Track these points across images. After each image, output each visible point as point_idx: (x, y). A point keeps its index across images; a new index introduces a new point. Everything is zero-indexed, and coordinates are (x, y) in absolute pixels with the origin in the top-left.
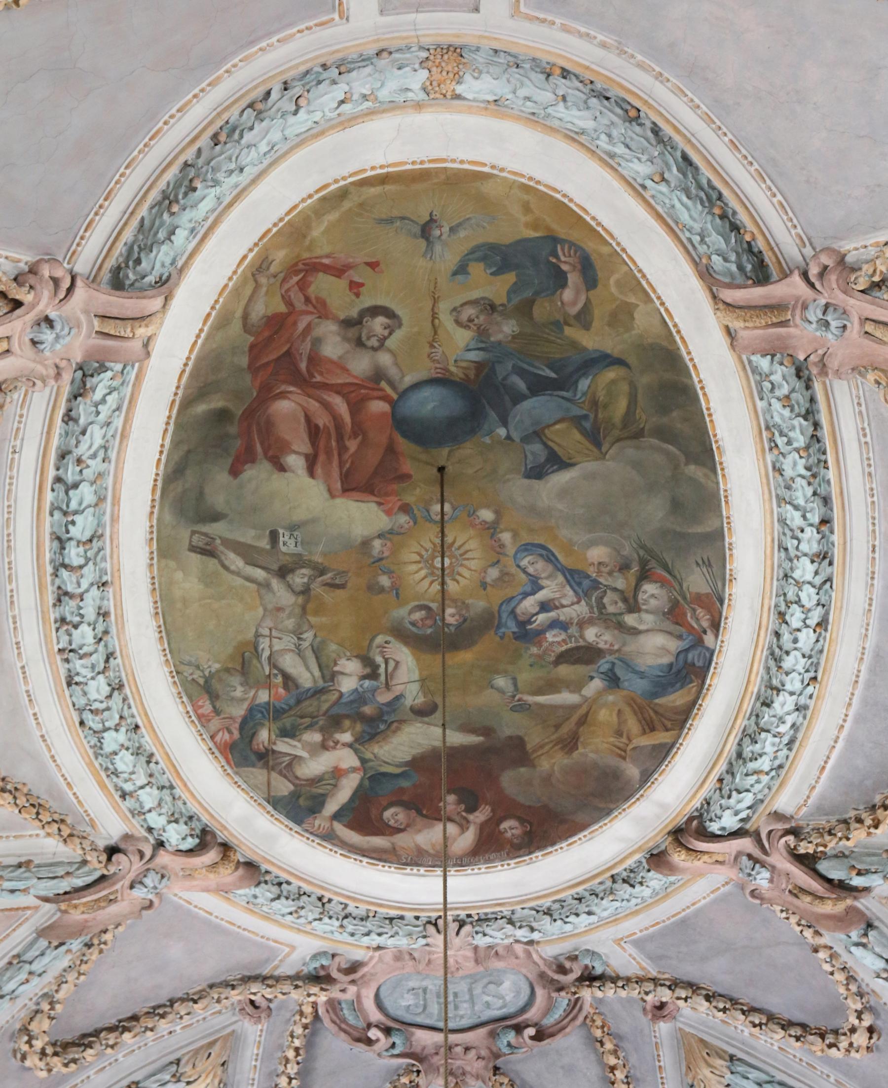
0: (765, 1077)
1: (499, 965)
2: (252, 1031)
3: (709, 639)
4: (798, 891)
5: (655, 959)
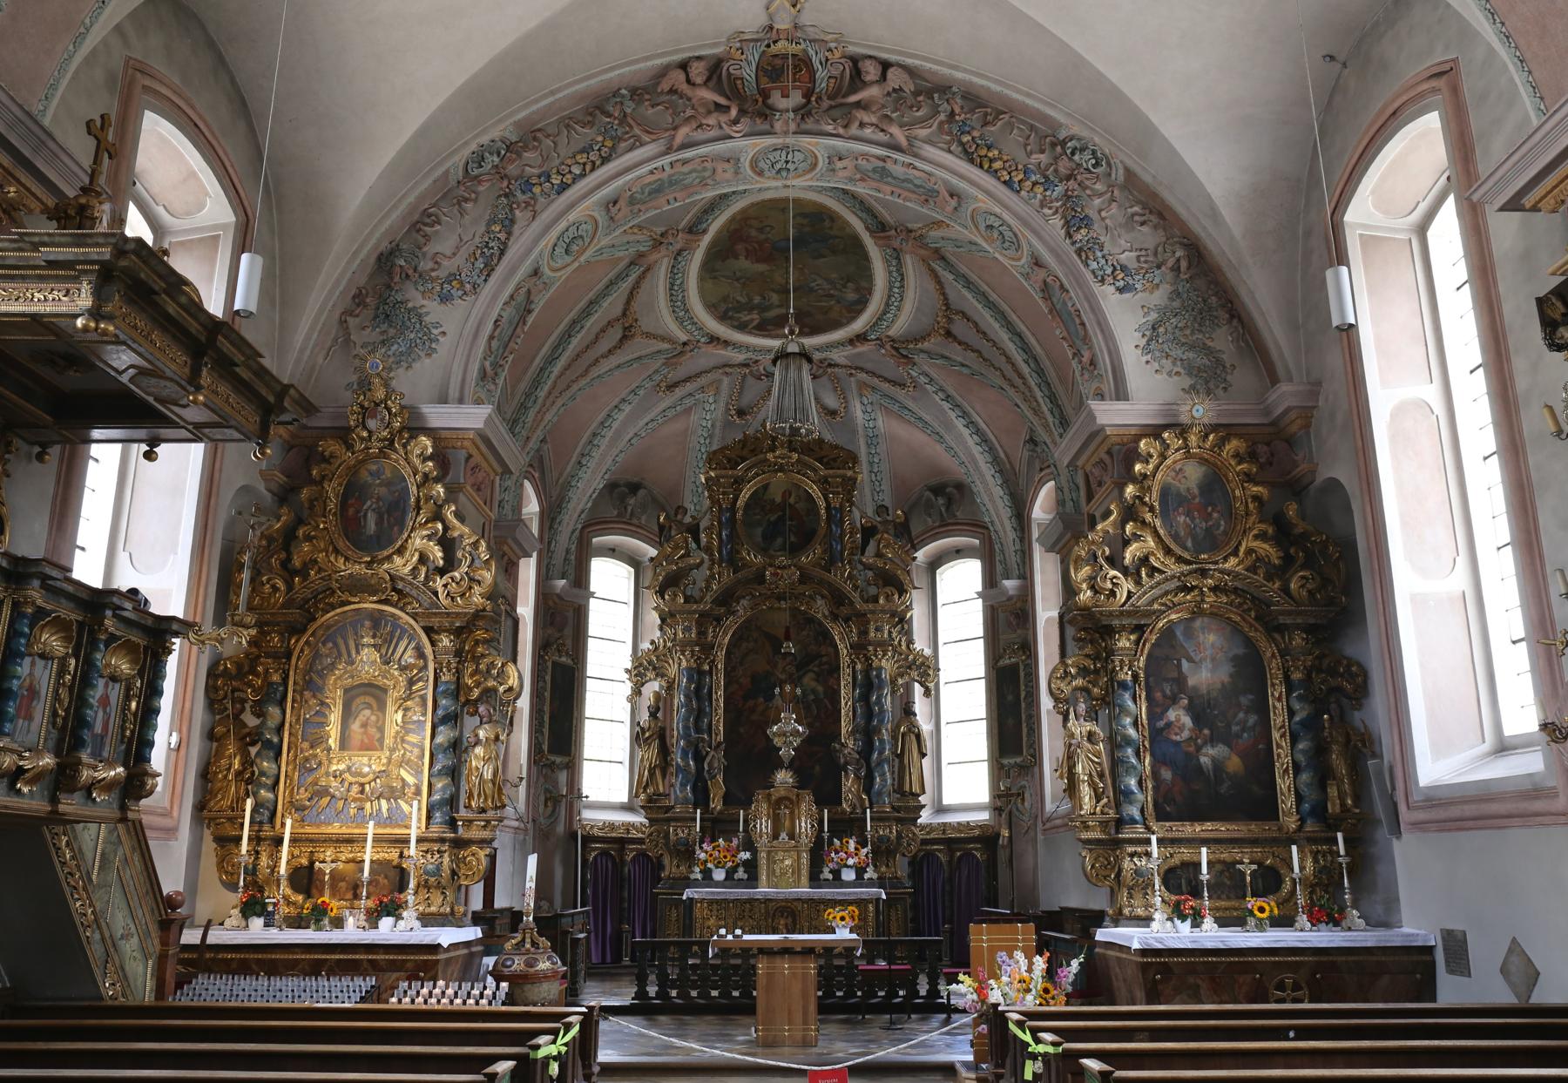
2: (726, 380)
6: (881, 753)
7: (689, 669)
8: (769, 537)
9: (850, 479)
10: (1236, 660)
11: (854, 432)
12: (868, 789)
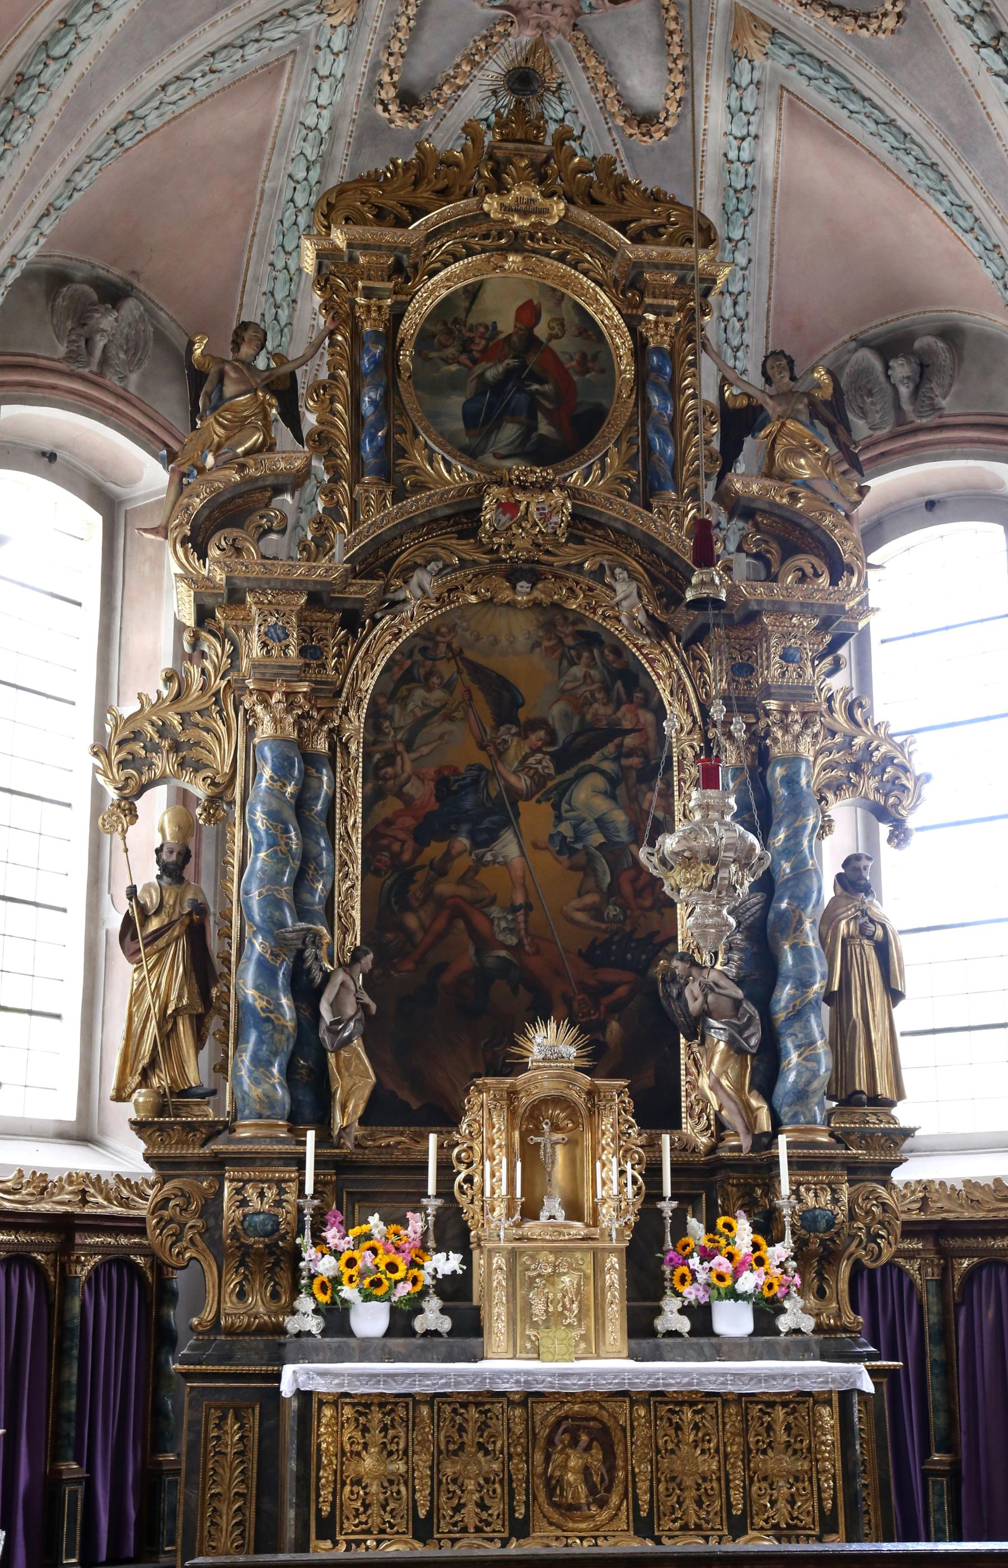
0: (798, 49)
6: (803, 984)
7: (279, 741)
8: (481, 421)
11: (695, 176)
12: (766, 1080)
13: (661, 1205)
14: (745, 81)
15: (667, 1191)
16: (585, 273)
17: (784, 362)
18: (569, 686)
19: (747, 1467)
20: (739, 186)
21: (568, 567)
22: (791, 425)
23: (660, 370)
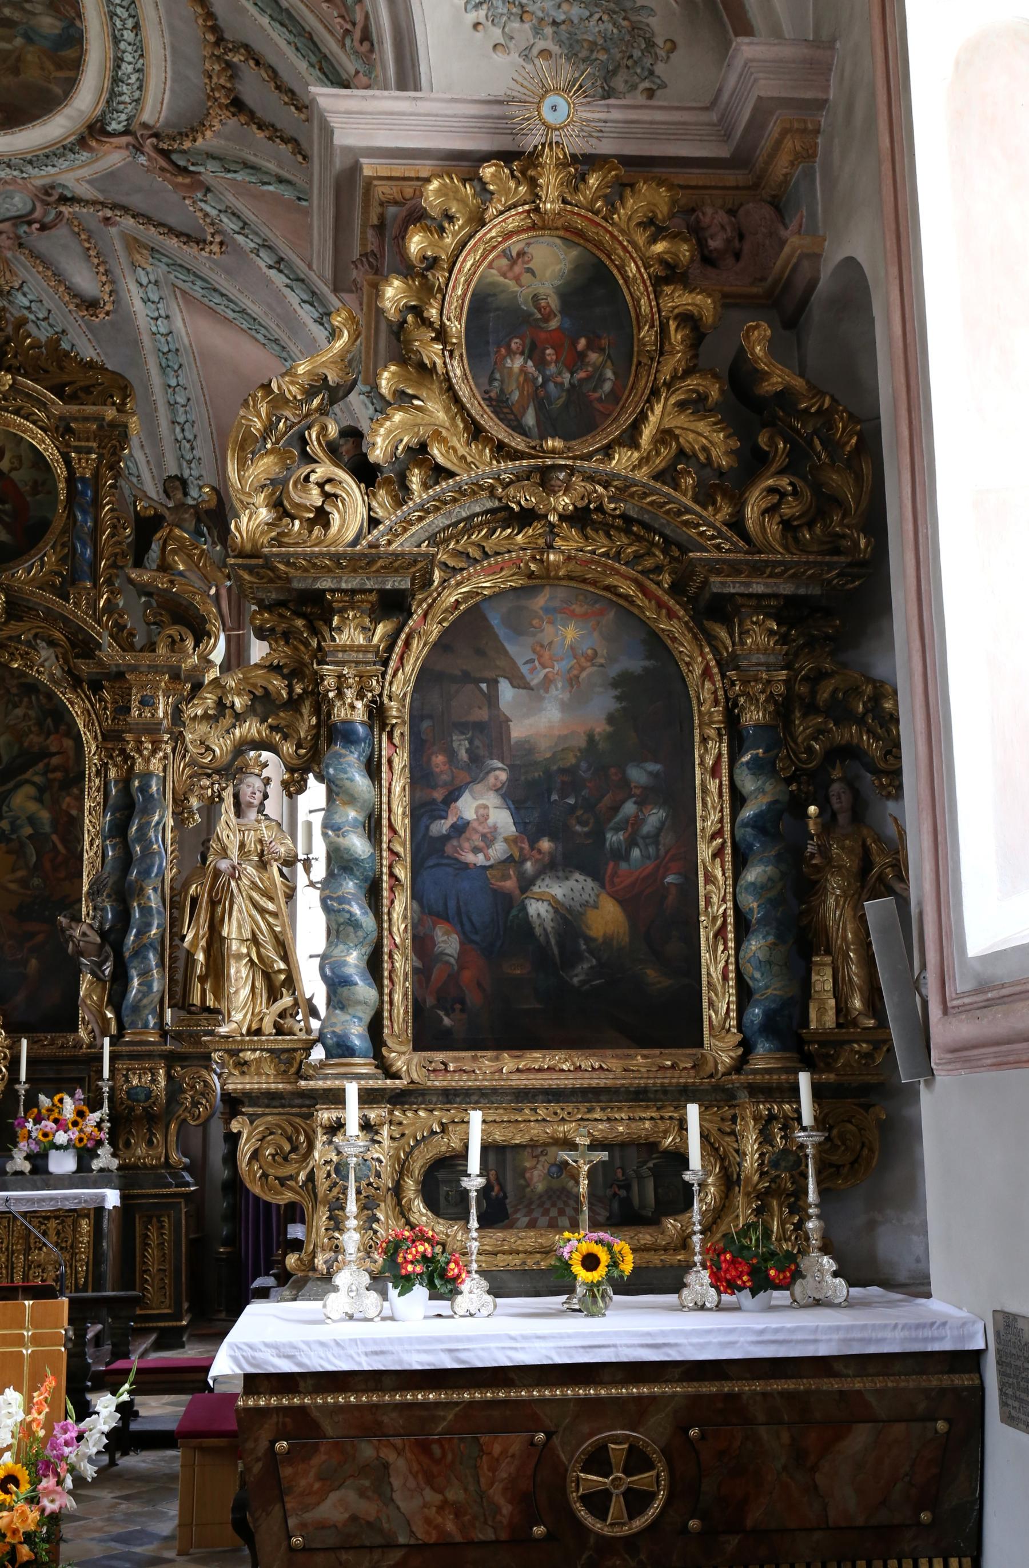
1: (11, 188)
3: (78, 23)
4: (162, 169)
5: (101, 191)
6: (141, 933)
9: (113, 425)
10: (623, 683)
11: (136, 344)
12: (117, 1000)
13: (17, 1086)
14: (145, 281)
15: (23, 1077)
16: (34, 423)
17: (177, 483)
18: (12, 723)
19: (26, 1259)
20: (166, 350)
21: (10, 638)
22: (177, 532)
23: (84, 494)
